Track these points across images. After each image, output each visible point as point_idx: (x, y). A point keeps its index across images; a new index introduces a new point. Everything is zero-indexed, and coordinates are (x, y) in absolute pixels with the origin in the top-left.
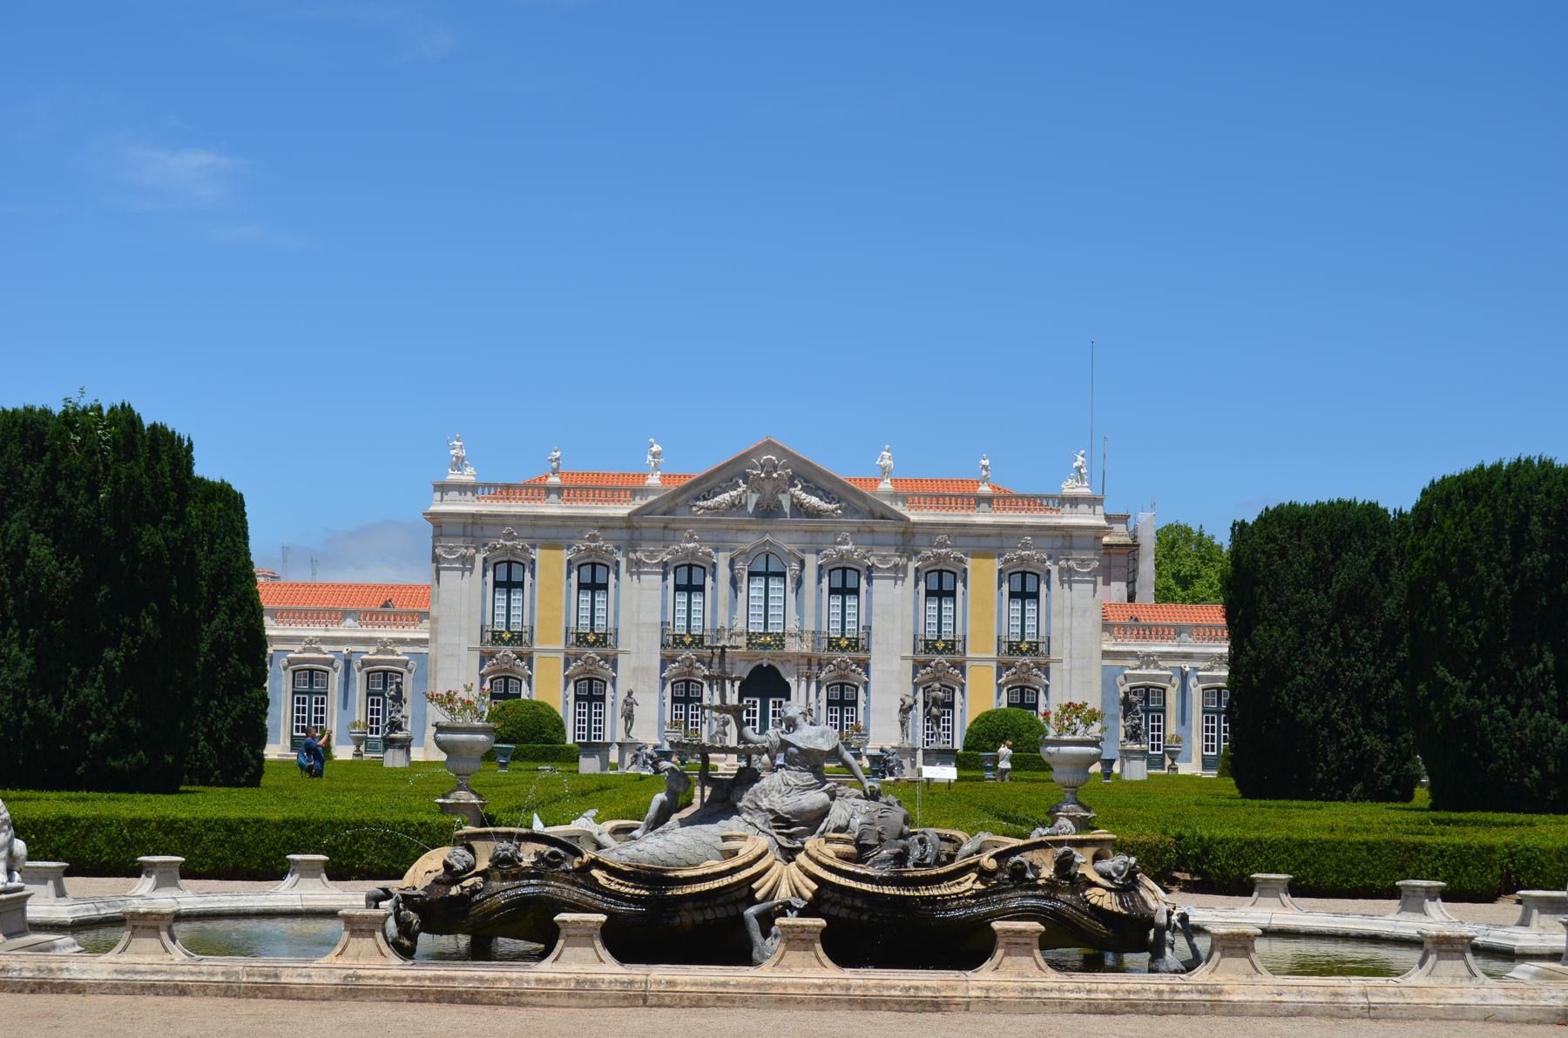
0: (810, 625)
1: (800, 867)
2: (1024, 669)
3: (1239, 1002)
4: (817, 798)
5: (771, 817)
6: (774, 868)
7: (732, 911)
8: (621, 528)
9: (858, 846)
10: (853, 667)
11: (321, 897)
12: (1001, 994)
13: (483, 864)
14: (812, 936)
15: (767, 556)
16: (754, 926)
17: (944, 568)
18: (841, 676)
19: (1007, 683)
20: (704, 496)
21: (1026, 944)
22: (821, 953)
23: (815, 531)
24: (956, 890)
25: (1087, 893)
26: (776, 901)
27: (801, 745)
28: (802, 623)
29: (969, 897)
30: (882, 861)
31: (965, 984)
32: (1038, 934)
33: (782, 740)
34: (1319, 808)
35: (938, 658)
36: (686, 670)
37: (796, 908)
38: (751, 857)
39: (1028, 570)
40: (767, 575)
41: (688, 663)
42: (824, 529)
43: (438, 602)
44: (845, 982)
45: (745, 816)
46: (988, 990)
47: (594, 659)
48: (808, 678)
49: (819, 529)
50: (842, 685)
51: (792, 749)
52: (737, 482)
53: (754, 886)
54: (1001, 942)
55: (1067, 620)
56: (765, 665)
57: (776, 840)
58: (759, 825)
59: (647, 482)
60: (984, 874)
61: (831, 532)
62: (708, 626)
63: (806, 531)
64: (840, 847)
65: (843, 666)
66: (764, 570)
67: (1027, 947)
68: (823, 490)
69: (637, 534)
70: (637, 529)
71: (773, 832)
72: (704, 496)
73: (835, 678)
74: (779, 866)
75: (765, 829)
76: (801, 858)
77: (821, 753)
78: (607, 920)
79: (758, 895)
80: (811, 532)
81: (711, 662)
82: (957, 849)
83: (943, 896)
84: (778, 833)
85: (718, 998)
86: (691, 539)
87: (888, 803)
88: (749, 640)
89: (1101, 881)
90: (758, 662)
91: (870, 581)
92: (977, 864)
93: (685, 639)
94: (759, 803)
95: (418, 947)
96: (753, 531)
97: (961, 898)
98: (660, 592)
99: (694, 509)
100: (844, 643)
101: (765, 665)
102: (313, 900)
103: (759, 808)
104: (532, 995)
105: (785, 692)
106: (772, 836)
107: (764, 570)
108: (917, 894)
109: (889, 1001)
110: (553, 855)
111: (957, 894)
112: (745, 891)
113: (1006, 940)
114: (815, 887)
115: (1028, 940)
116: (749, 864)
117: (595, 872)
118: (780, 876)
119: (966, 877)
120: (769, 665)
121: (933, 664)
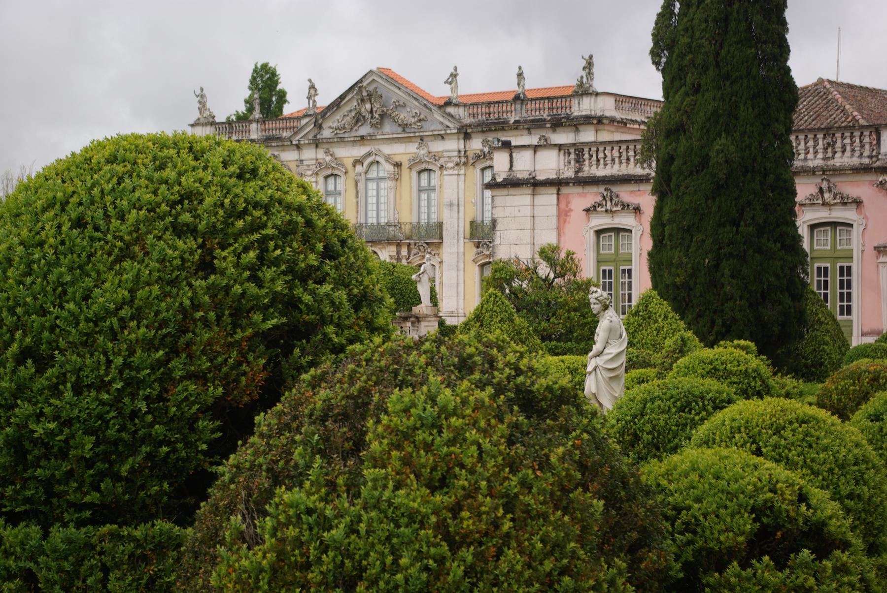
40: (379, 179)
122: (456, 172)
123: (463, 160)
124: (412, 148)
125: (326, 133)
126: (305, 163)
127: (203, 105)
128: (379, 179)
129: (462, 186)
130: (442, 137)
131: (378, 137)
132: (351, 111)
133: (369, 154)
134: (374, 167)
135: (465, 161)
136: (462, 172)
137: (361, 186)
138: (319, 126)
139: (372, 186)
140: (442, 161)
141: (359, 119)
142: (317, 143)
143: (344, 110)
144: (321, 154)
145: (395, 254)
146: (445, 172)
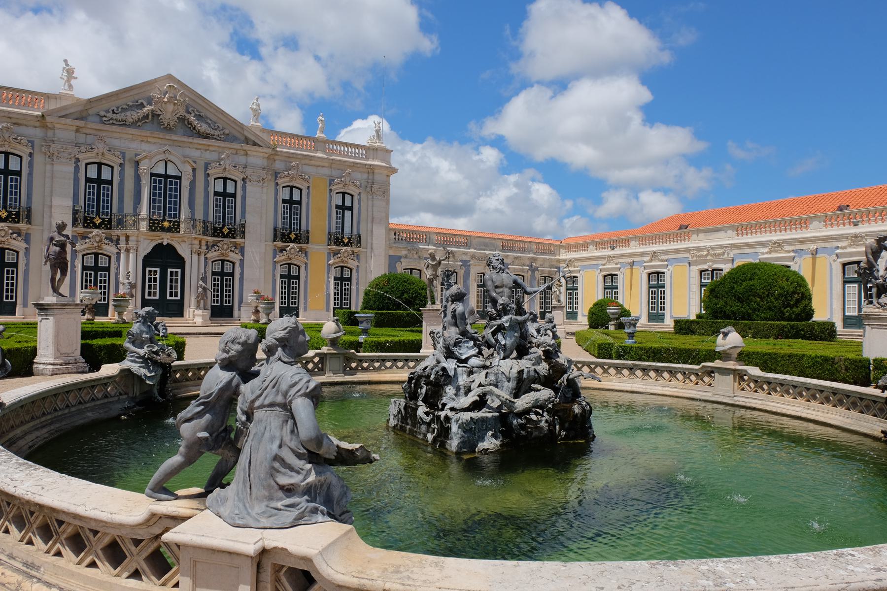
0: (199, 215)
2: (346, 255)
8: (35, 127)
10: (233, 249)
15: (166, 163)
17: (295, 185)
18: (223, 255)
19: (334, 263)
20: (113, 111)
23: (203, 149)
28: (193, 212)
35: (291, 245)
36: (96, 244)
39: (348, 191)
40: (166, 176)
41: (98, 239)
42: (211, 148)
47: (6, 233)
48: (199, 254)
49: (207, 148)
50: (223, 261)
52: (142, 104)
55: (370, 225)
56: (165, 244)
61: (215, 151)
62: (115, 211)
63: (196, 149)
65: (225, 247)
66: (164, 173)
68: (210, 120)
69: (50, 133)
70: (50, 128)
72: (113, 111)
73: (219, 256)
80: (201, 149)
81: (118, 240)
88: (154, 223)
91: (244, 187)
93: (95, 220)
96: (154, 143)
98: (72, 182)
99: (104, 119)
100: (226, 231)
101: (165, 244)
105: (180, 262)
107: (164, 173)
120: (168, 244)
121: (288, 249)
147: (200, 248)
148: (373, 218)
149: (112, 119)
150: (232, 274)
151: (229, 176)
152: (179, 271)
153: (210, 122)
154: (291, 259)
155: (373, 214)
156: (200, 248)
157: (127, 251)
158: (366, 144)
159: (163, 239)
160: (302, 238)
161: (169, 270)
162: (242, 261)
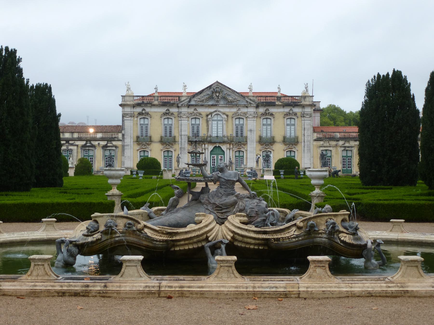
1: (226, 227)
3: (416, 291)
4: (232, 199)
5: (215, 206)
6: (216, 227)
7: (200, 245)
9: (247, 216)
11: (54, 234)
12: (313, 290)
13: (102, 228)
14: (231, 265)
16: (208, 251)
18: (239, 148)
19: (286, 150)
21: (323, 266)
22: (235, 272)
24: (287, 235)
25: (340, 235)
26: (216, 241)
27: (226, 178)
29: (293, 238)
30: (258, 222)
31: (297, 285)
32: (328, 263)
33: (218, 176)
34: (391, 189)
37: (225, 243)
38: (207, 223)
40: (218, 120)
43: (124, 130)
44: (245, 285)
45: (205, 206)
46: (307, 288)
48: (230, 149)
51: (223, 180)
53: (208, 235)
54: (310, 262)
55: (303, 131)
56: (217, 146)
57: (217, 215)
58: (210, 210)
59: (183, 94)
60: (299, 228)
64: (242, 218)
67: (324, 268)
71: (215, 212)
74: (218, 225)
75: (212, 210)
76: (226, 223)
77: (234, 181)
78: (143, 259)
79: (210, 239)
82: (286, 216)
83: (282, 238)
84: (217, 212)
85: (191, 293)
86: (195, 109)
87: (259, 200)
89: (345, 231)
90: (215, 145)
92: (295, 225)
94: (210, 201)
95: (77, 262)
97: (290, 238)
99: (196, 102)
101: (217, 146)
102: (51, 235)
103: (210, 203)
104: (110, 293)
106: (215, 213)
108: (272, 237)
109: (265, 293)
110: (129, 224)
111: (288, 237)
112: (205, 236)
113: (314, 265)
114: (232, 235)
115: (324, 265)
116: (206, 226)
117: (146, 230)
118: (218, 230)
119: (291, 230)
122: (253, 119)
123: (256, 115)
124: (234, 110)
125: (193, 103)
126: (182, 113)
127: (128, 89)
128: (218, 120)
129: (255, 124)
130: (247, 107)
131: (219, 105)
132: (205, 95)
133: (216, 111)
134: (216, 116)
135: (256, 116)
136: (255, 119)
137: (210, 122)
138: (190, 101)
139: (214, 122)
140: (248, 115)
141: (211, 98)
142: (189, 106)
143: (202, 95)
144: (191, 110)
145: (229, 147)
146: (248, 119)
147: (230, 147)
148: (304, 128)
149: (199, 101)
150: (243, 157)
151: (240, 117)
152: (223, 156)
153: (232, 97)
154: (267, 149)
155: (304, 127)
156: (230, 147)
157: (205, 149)
158: (300, 95)
159: (216, 144)
160: (262, 141)
161: (219, 156)
162: (247, 150)
